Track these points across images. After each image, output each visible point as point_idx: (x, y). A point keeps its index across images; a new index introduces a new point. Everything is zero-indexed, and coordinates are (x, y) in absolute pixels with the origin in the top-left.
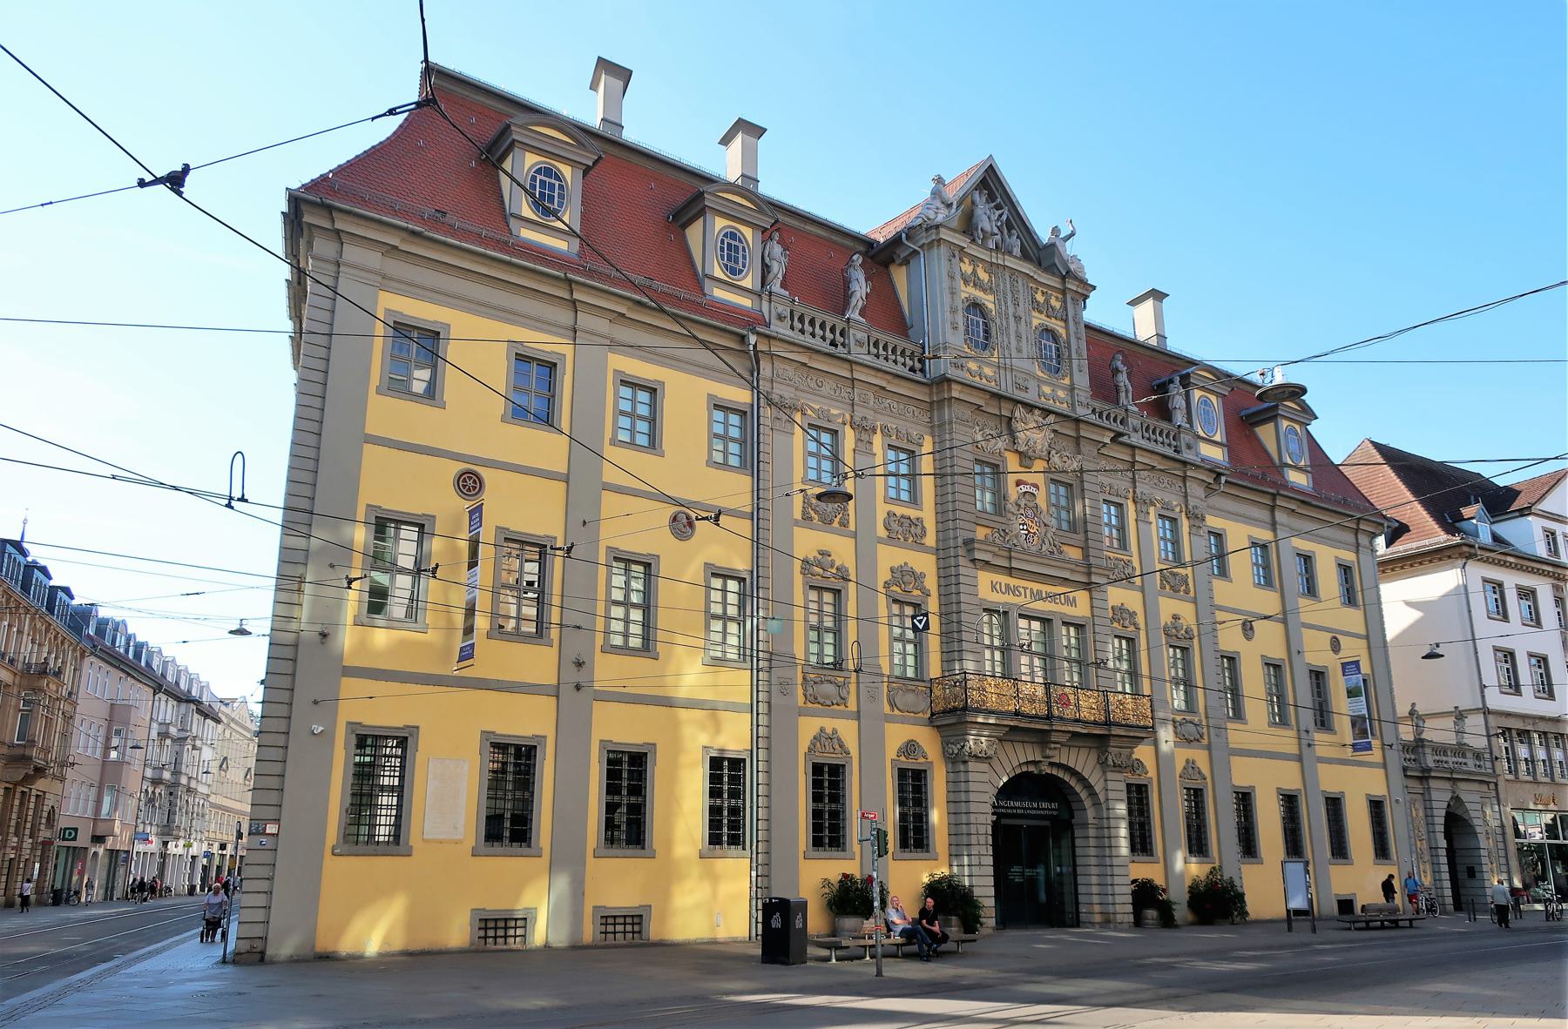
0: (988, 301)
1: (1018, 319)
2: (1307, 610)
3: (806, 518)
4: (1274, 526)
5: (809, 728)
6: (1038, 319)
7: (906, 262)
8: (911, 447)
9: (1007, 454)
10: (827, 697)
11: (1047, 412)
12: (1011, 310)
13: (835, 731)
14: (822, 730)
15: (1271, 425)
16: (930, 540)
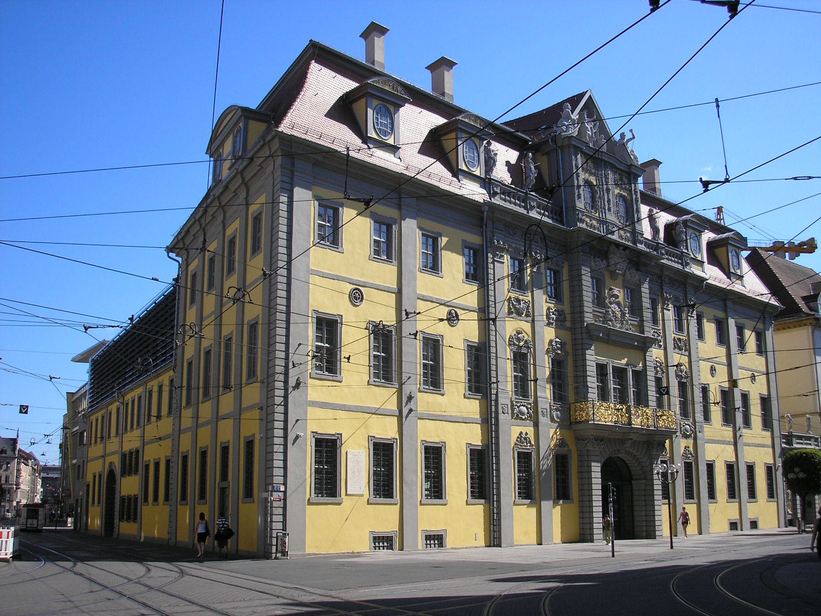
0: (593, 180)
1: (608, 190)
2: (739, 360)
3: (510, 313)
4: (725, 311)
5: (515, 431)
6: (617, 191)
7: (547, 154)
8: (557, 268)
9: (605, 272)
10: (523, 414)
11: (626, 248)
12: (605, 187)
13: (526, 434)
14: (521, 433)
15: (724, 248)
16: (568, 324)
